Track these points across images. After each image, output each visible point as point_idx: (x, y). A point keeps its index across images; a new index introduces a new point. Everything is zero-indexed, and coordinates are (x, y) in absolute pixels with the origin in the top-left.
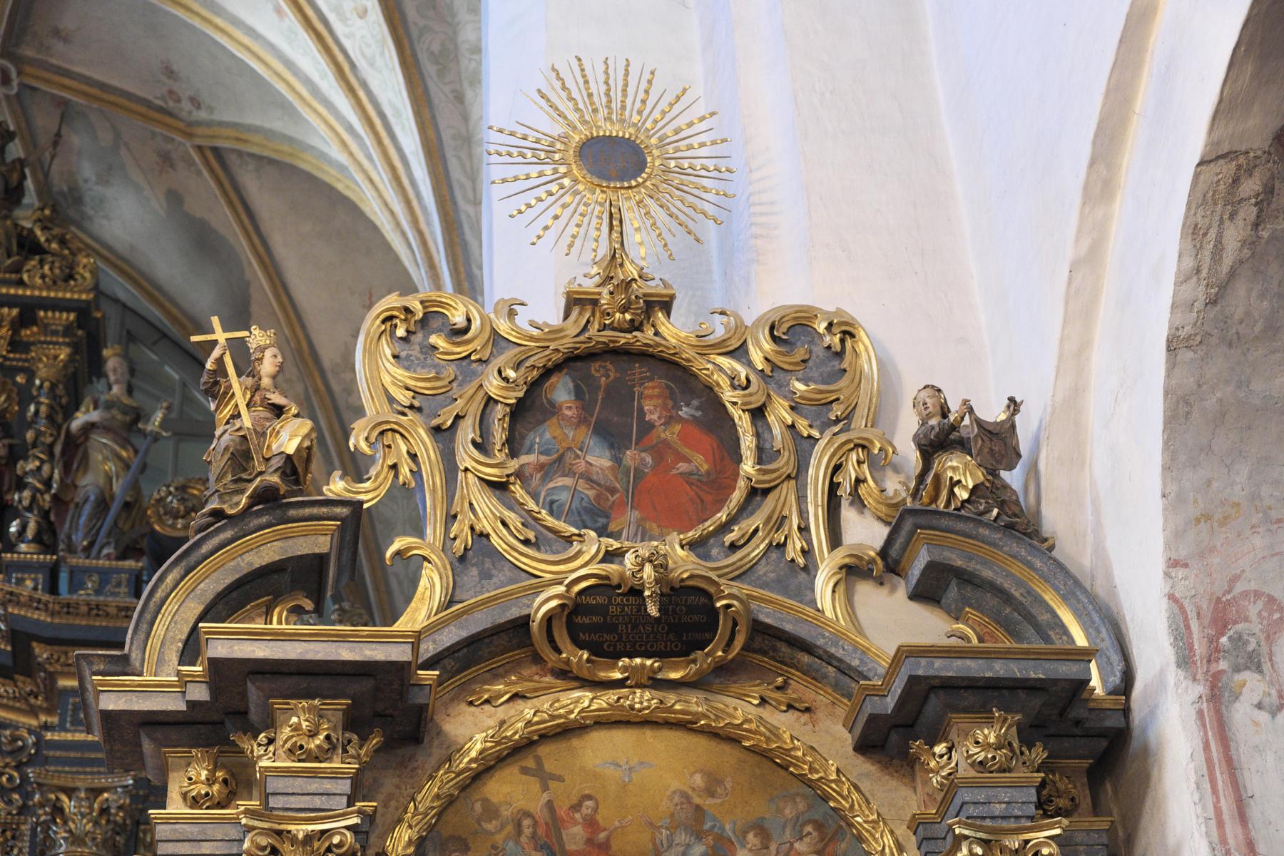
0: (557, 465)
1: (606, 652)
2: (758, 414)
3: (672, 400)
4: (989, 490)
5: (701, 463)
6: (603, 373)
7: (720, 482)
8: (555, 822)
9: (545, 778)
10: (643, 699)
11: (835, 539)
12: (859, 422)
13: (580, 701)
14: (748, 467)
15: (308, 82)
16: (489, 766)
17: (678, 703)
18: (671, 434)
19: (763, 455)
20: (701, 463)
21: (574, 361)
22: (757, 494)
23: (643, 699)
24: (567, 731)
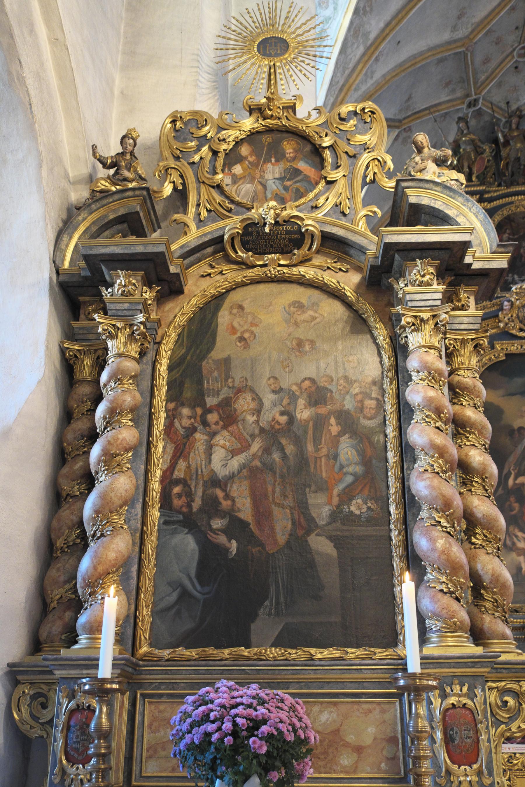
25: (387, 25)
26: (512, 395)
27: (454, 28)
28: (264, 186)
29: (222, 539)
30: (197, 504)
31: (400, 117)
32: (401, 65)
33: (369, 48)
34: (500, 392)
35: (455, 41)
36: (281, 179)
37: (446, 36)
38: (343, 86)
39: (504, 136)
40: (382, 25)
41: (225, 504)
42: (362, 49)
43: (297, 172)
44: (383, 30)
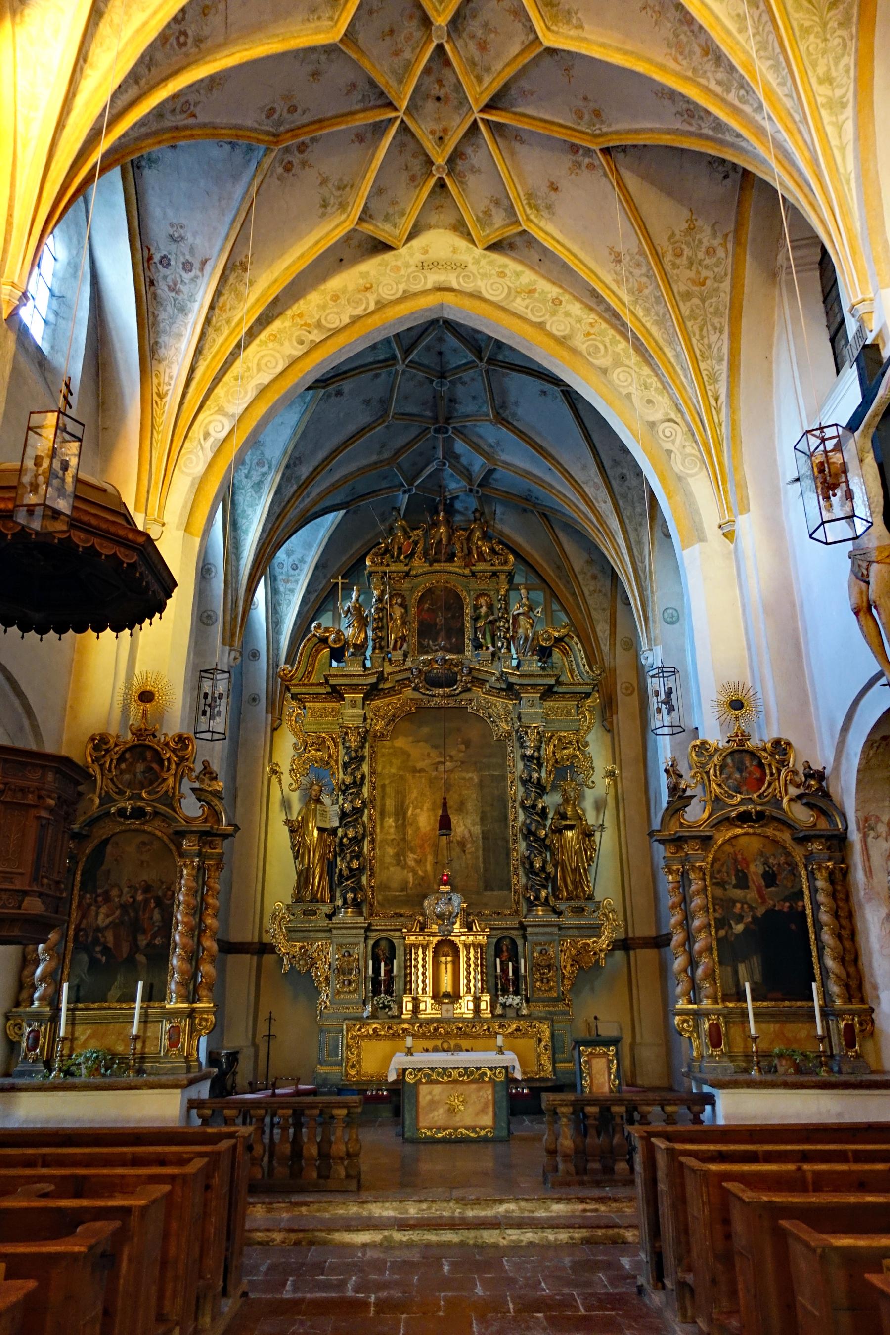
0: (728, 778)
1: (745, 823)
2: (770, 766)
3: (751, 760)
4: (820, 788)
5: (758, 775)
6: (737, 756)
7: (761, 781)
8: (736, 855)
9: (733, 846)
10: (751, 830)
11: (786, 794)
12: (791, 765)
13: (739, 831)
14: (768, 778)
15: (584, 513)
16: (722, 844)
17: (758, 831)
18: (752, 769)
19: (772, 774)
20: (758, 775)
21: (731, 753)
22: (770, 784)
23: (751, 830)
24: (736, 836)
25: (315, 470)
26: (418, 741)
27: (380, 453)
28: (135, 775)
29: (99, 956)
30: (90, 940)
31: (348, 499)
32: (333, 484)
33: (300, 487)
34: (411, 739)
35: (381, 461)
36: (144, 772)
37: (374, 458)
38: (279, 515)
39: (432, 519)
40: (311, 469)
41: (102, 940)
42: (295, 487)
43: (152, 769)
44: (312, 473)
